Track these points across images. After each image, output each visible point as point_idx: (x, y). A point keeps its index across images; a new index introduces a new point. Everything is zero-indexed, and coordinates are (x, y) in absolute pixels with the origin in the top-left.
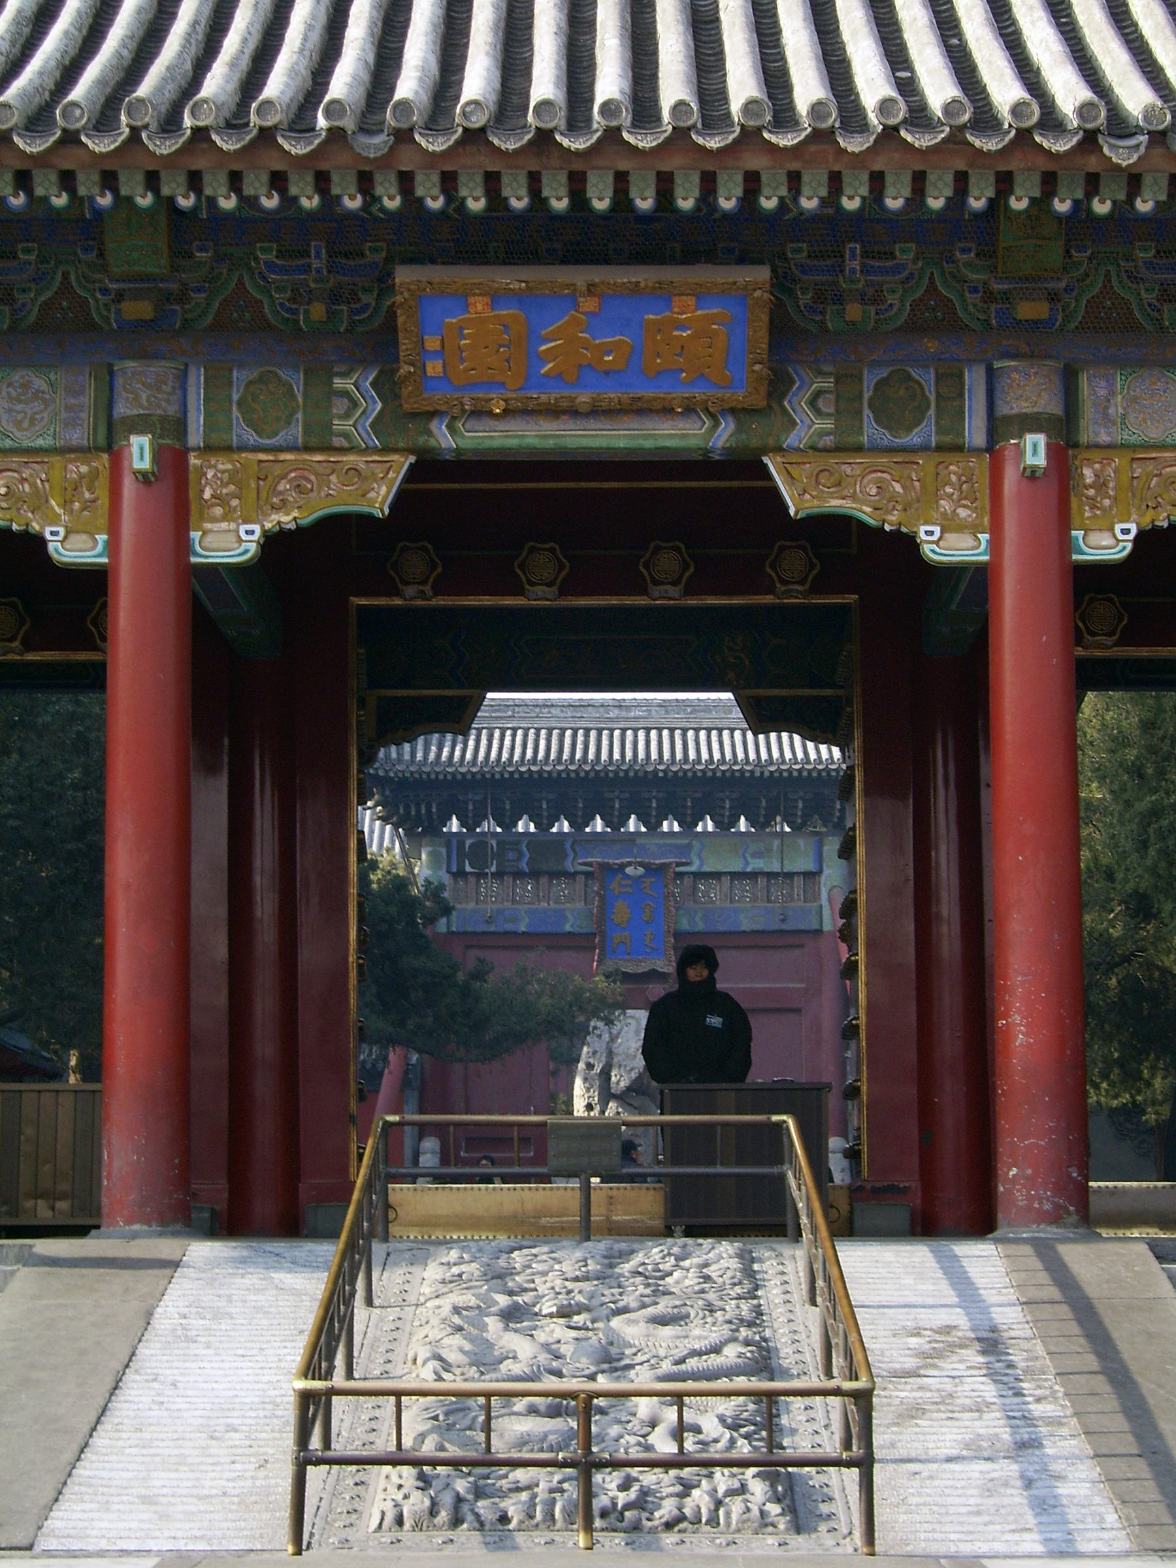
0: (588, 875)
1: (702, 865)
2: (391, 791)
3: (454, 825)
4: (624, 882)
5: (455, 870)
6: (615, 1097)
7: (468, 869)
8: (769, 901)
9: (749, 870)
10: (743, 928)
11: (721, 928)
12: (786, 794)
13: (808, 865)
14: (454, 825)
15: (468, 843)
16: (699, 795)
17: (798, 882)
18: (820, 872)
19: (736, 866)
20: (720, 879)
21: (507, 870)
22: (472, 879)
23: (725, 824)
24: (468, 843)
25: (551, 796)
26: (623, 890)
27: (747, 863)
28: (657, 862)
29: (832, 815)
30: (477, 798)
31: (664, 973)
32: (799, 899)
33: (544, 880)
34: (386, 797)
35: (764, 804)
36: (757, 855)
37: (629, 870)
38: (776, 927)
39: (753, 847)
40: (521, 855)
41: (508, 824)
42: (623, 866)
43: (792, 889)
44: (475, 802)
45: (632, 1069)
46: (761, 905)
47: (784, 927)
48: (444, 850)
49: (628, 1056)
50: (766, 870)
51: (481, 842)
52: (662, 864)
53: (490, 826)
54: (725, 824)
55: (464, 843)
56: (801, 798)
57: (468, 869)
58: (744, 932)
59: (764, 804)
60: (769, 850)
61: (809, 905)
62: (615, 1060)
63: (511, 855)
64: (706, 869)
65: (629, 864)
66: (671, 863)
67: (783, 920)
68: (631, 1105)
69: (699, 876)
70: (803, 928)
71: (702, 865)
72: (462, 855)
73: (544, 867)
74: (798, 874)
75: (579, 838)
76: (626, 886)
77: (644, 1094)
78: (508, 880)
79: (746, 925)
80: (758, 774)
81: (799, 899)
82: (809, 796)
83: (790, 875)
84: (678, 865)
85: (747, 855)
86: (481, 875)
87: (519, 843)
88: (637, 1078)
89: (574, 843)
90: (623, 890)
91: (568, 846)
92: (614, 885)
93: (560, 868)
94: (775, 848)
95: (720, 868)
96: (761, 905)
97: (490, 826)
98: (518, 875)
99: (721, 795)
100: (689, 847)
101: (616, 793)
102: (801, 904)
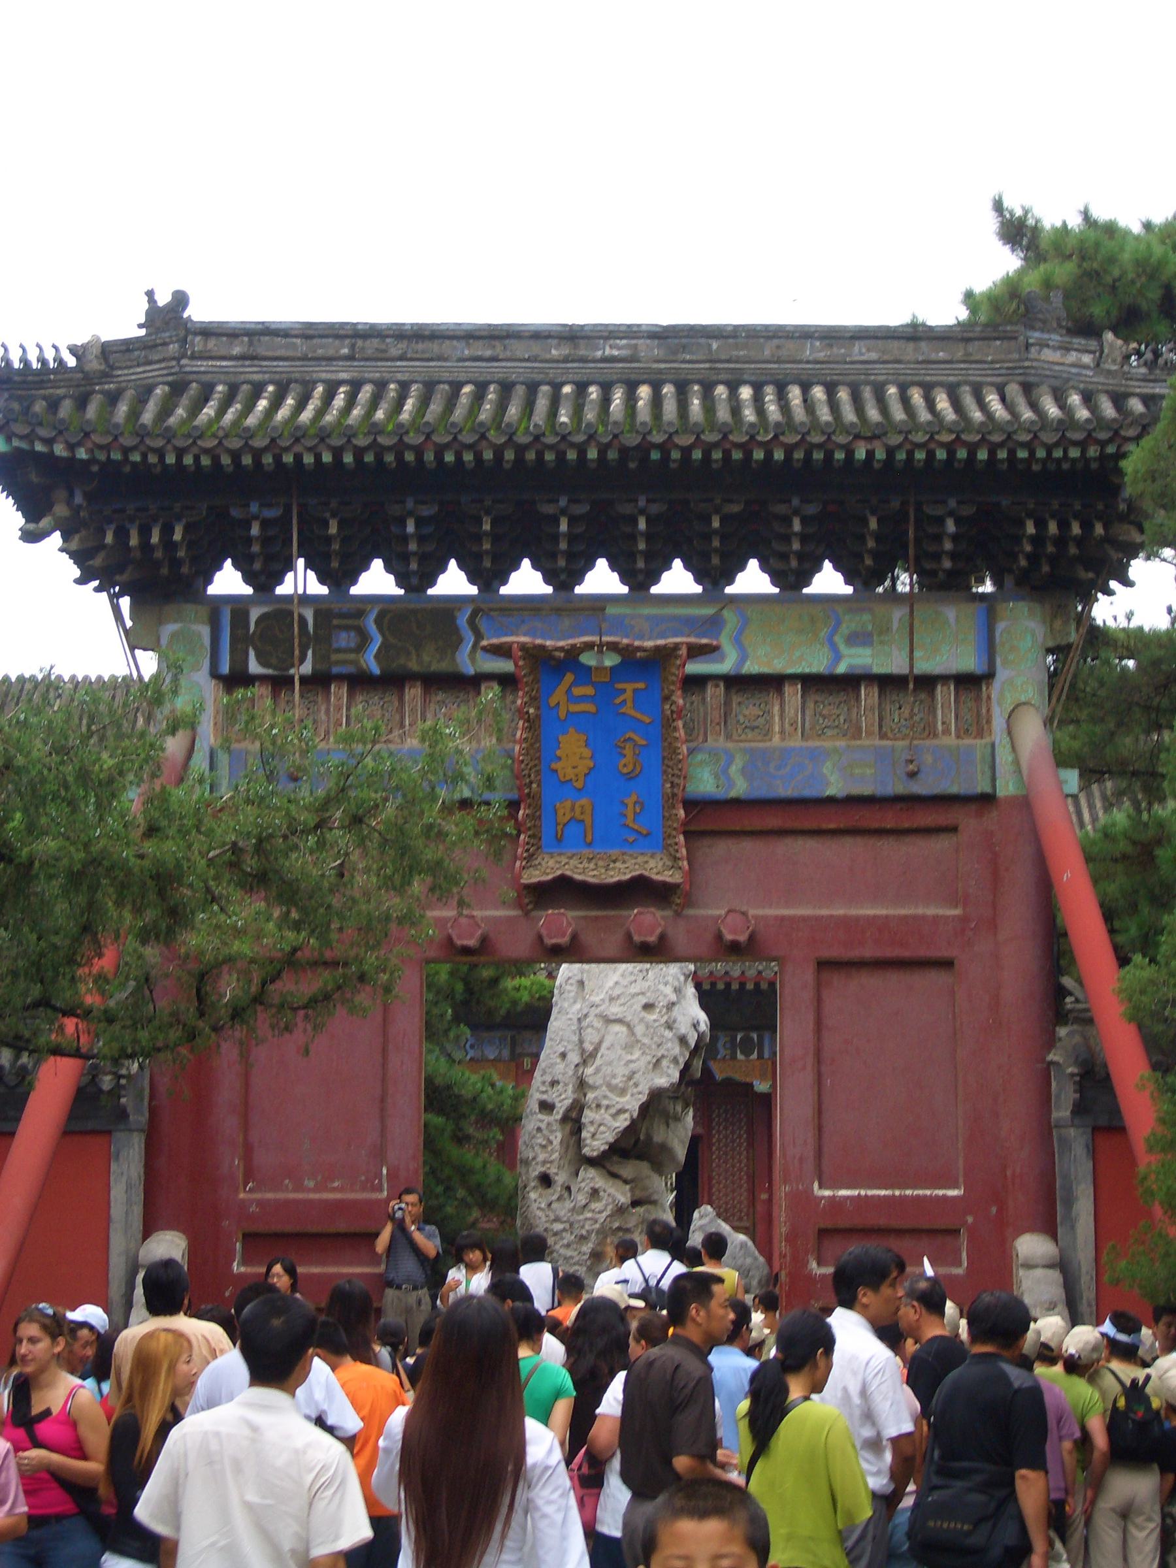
0: (507, 681)
1: (743, 659)
2: (88, 496)
3: (228, 581)
4: (578, 691)
5: (225, 669)
6: (592, 1162)
7: (254, 667)
8: (883, 736)
9: (841, 669)
10: (830, 792)
11: (784, 790)
12: (919, 508)
13: (967, 661)
14: (228, 581)
15: (255, 614)
16: (735, 508)
17: (944, 695)
18: (990, 676)
19: (816, 662)
20: (780, 690)
21: (335, 670)
22: (261, 691)
23: (791, 576)
24: (255, 614)
25: (426, 511)
26: (575, 708)
27: (838, 657)
28: (649, 644)
29: (1014, 556)
30: (270, 513)
31: (664, 884)
32: (947, 732)
33: (413, 693)
34: (76, 510)
35: (873, 524)
36: (858, 638)
37: (588, 659)
38: (899, 787)
39: (850, 624)
40: (364, 639)
41: (340, 574)
42: (573, 653)
43: (932, 710)
44: (265, 523)
45: (621, 1111)
46: (866, 742)
47: (918, 788)
48: (205, 631)
49: (610, 1086)
50: (877, 670)
51: (283, 612)
52: (657, 649)
53: (301, 581)
54: (791, 576)
55: (246, 615)
56: (951, 514)
57: (254, 667)
58: (831, 800)
59: (873, 524)
60: (884, 630)
61: (967, 741)
62: (590, 1096)
63: (344, 639)
64: (752, 667)
65: (589, 646)
66: (677, 646)
67: (912, 775)
68: (614, 1175)
69: (737, 683)
70: (954, 789)
71: (743, 659)
72: (240, 641)
73: (414, 666)
74: (944, 678)
75: (490, 606)
76: (583, 698)
77: (640, 1157)
78: (338, 692)
79: (835, 786)
80: (861, 454)
81: (947, 732)
82: (968, 511)
83: (927, 683)
84: (696, 652)
85: (838, 639)
86: (280, 683)
87: (361, 614)
88: (627, 1130)
89: (475, 614)
90: (575, 708)
91: (462, 620)
92: (558, 696)
93: (443, 666)
94: (895, 625)
95: (778, 666)
96: (866, 742)
97: (301, 581)
98: (360, 682)
99: (781, 509)
100: (714, 624)
101: (563, 502)
102: (950, 740)
